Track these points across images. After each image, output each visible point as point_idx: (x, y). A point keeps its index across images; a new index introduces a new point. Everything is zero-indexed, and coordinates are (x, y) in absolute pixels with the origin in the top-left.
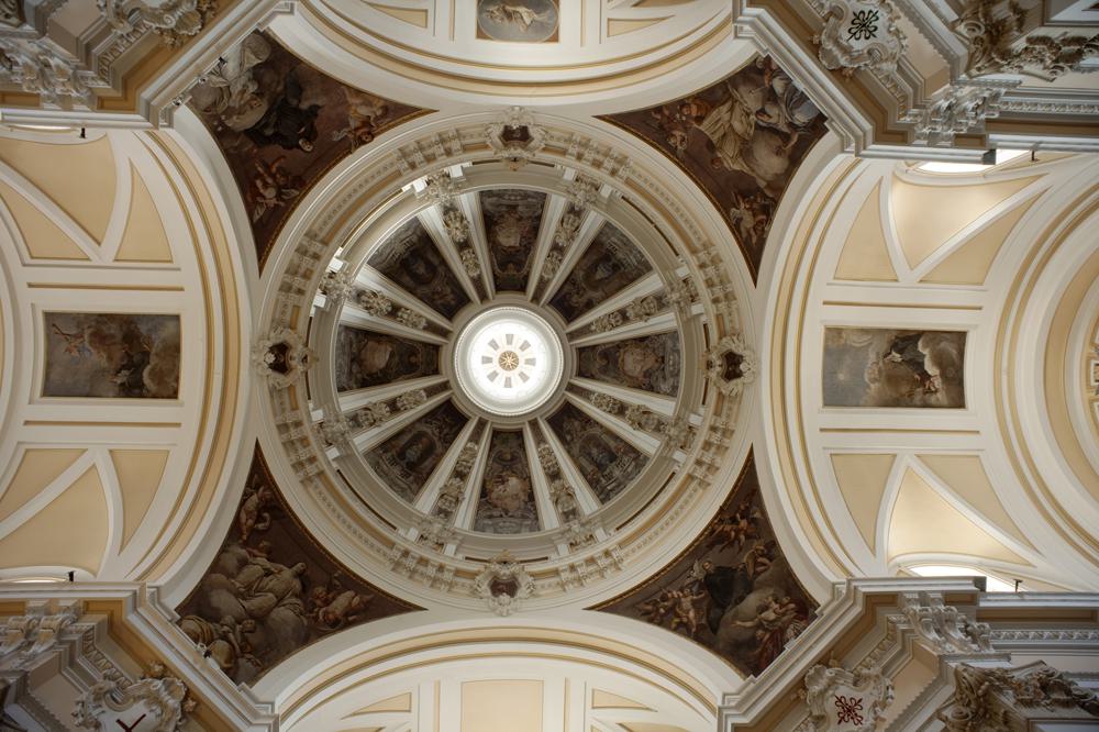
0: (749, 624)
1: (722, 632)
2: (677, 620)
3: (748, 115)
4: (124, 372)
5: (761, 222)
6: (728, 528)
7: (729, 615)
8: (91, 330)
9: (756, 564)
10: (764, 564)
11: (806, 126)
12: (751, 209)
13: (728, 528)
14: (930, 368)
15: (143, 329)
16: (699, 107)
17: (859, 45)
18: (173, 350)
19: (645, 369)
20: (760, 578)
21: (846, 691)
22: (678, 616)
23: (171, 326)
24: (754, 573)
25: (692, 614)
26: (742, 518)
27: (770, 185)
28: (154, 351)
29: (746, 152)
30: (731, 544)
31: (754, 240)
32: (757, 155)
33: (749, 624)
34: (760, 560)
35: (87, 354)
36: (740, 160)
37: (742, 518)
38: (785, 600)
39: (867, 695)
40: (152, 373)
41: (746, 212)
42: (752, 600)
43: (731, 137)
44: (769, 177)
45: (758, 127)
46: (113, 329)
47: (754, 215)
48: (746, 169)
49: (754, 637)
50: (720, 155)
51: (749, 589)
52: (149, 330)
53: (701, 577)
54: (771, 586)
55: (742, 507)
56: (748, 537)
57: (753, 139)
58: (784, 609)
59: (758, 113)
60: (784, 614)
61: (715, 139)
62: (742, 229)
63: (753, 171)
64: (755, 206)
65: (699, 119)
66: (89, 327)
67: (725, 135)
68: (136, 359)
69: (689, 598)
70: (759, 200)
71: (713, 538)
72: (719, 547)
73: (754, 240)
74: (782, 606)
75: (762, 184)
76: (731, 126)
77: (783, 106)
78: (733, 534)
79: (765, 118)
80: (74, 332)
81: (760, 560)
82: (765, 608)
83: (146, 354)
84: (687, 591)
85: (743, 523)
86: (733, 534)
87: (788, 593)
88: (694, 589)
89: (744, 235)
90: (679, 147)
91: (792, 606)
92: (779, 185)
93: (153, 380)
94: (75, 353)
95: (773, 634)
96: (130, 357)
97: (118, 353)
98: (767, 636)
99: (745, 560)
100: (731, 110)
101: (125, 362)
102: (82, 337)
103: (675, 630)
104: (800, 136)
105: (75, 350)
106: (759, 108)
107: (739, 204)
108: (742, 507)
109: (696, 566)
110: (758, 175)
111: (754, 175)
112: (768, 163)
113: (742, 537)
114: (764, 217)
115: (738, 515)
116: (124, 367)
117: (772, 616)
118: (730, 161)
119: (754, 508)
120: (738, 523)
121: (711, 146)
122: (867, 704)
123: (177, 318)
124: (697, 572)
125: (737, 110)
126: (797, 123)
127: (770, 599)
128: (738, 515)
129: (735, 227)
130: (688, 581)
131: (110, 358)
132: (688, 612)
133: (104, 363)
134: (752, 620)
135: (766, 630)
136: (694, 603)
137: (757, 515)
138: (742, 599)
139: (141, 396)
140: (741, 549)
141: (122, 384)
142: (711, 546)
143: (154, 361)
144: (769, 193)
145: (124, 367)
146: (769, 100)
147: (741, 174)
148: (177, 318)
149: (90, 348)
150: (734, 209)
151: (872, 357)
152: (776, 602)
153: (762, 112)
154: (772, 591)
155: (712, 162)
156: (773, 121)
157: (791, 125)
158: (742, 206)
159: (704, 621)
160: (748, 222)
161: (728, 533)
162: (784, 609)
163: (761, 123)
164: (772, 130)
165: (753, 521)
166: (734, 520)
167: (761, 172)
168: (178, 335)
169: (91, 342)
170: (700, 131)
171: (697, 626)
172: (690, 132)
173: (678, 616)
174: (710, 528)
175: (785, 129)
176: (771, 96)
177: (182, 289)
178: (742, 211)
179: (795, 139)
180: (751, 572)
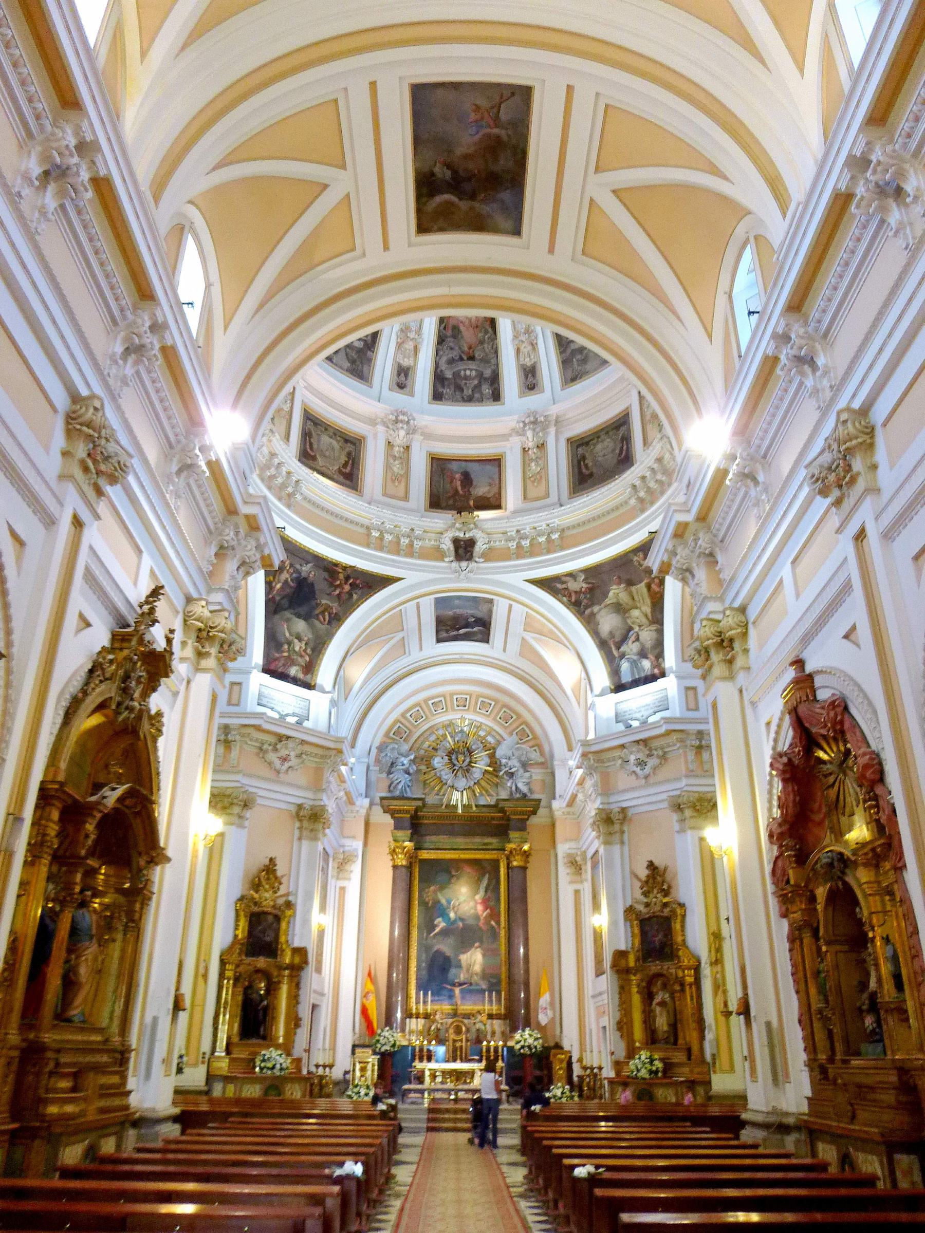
0: (287, 634)
1: (277, 617)
2: (272, 578)
3: (640, 626)
4: (448, 173)
5: (570, 596)
6: (341, 576)
7: (287, 614)
8: (505, 138)
9: (323, 613)
10: (324, 619)
11: (619, 666)
12: (581, 592)
13: (341, 576)
14: (462, 631)
15: (506, 196)
16: (656, 593)
17: (632, 758)
18: (479, 225)
19: (462, 328)
20: (316, 622)
21: (293, 754)
22: (274, 578)
23: (509, 225)
24: (317, 615)
25: (279, 586)
26: (351, 585)
27: (593, 615)
28: (477, 205)
29: (619, 609)
30: (331, 585)
31: (559, 586)
32: (614, 615)
33: (287, 634)
34: (326, 614)
35: (473, 130)
36: (614, 600)
37: (351, 585)
38: (309, 651)
39: (294, 761)
40: (450, 203)
41: (579, 586)
42: (300, 625)
43: (631, 603)
44: (598, 617)
45: (630, 629)
46: (504, 163)
47: (576, 592)
48: (608, 601)
49: (281, 645)
50: (623, 586)
51: (307, 618)
52: (503, 202)
53: (304, 575)
54: (313, 633)
55: (358, 582)
56: (339, 595)
57: (624, 620)
58: (303, 653)
59: (638, 636)
60: (301, 656)
61: (633, 589)
62: (568, 579)
63: (605, 607)
64: (582, 596)
65: (649, 586)
66: (509, 136)
67: (633, 599)
68: (467, 187)
69: (288, 576)
70: (585, 601)
71: (331, 569)
72: (326, 575)
73: (559, 586)
74: (305, 651)
75: (596, 609)
76: (636, 608)
77: (635, 658)
78: (338, 582)
79: (633, 638)
80: (503, 116)
81: (326, 614)
82: (300, 639)
83: (473, 197)
84: (291, 570)
85: (347, 588)
86: (338, 582)
87: (313, 650)
88: (294, 575)
89: (564, 579)
90: (635, 558)
91: (307, 659)
92: (590, 622)
93: (440, 204)
94: (473, 116)
95: (288, 657)
96: (469, 179)
97: (473, 166)
98: (286, 654)
99: (324, 602)
100: (646, 616)
101: (461, 173)
102: (496, 126)
103: (266, 583)
104: (615, 657)
105: (478, 117)
106: (641, 638)
107: (587, 583)
108: (358, 582)
109: (310, 565)
110: (600, 610)
111: (602, 605)
112: (608, 622)
113: (337, 592)
114: (573, 600)
115: (351, 581)
116: (455, 172)
117: (297, 649)
118: (616, 592)
119: (359, 592)
120: (346, 583)
121: (630, 583)
122: (290, 764)
123: (517, 232)
124: (306, 569)
125: (644, 620)
126: (623, 661)
127: (306, 639)
128: (351, 581)
129: (571, 575)
130: (298, 566)
131: (466, 157)
132: (279, 582)
133: (459, 151)
134: (291, 634)
135: (289, 651)
136: (286, 582)
137: (355, 596)
138: (299, 616)
139: (419, 197)
140: (329, 594)
141: (433, 174)
142: (326, 569)
143: (464, 205)
144: (588, 612)
145: (455, 172)
146: (642, 650)
147: (605, 595)
148: (517, 232)
149: (481, 134)
150: (583, 577)
151: (472, 612)
152: (306, 644)
153: (637, 639)
154: (310, 636)
155: (619, 577)
156: (630, 642)
157: (622, 656)
158: (585, 585)
159: (278, 598)
160: (573, 586)
161: (337, 579)
162: (303, 653)
163: (631, 633)
164: (625, 639)
165: (351, 596)
166: (347, 578)
167: (603, 612)
168: (496, 230)
169: (488, 136)
170: (641, 582)
171: (273, 597)
172: (643, 574)
173: (274, 578)
174: (336, 565)
175: (622, 649)
176: (643, 654)
177: (551, 250)
178: (579, 585)
179: (615, 653)
180: (317, 612)
